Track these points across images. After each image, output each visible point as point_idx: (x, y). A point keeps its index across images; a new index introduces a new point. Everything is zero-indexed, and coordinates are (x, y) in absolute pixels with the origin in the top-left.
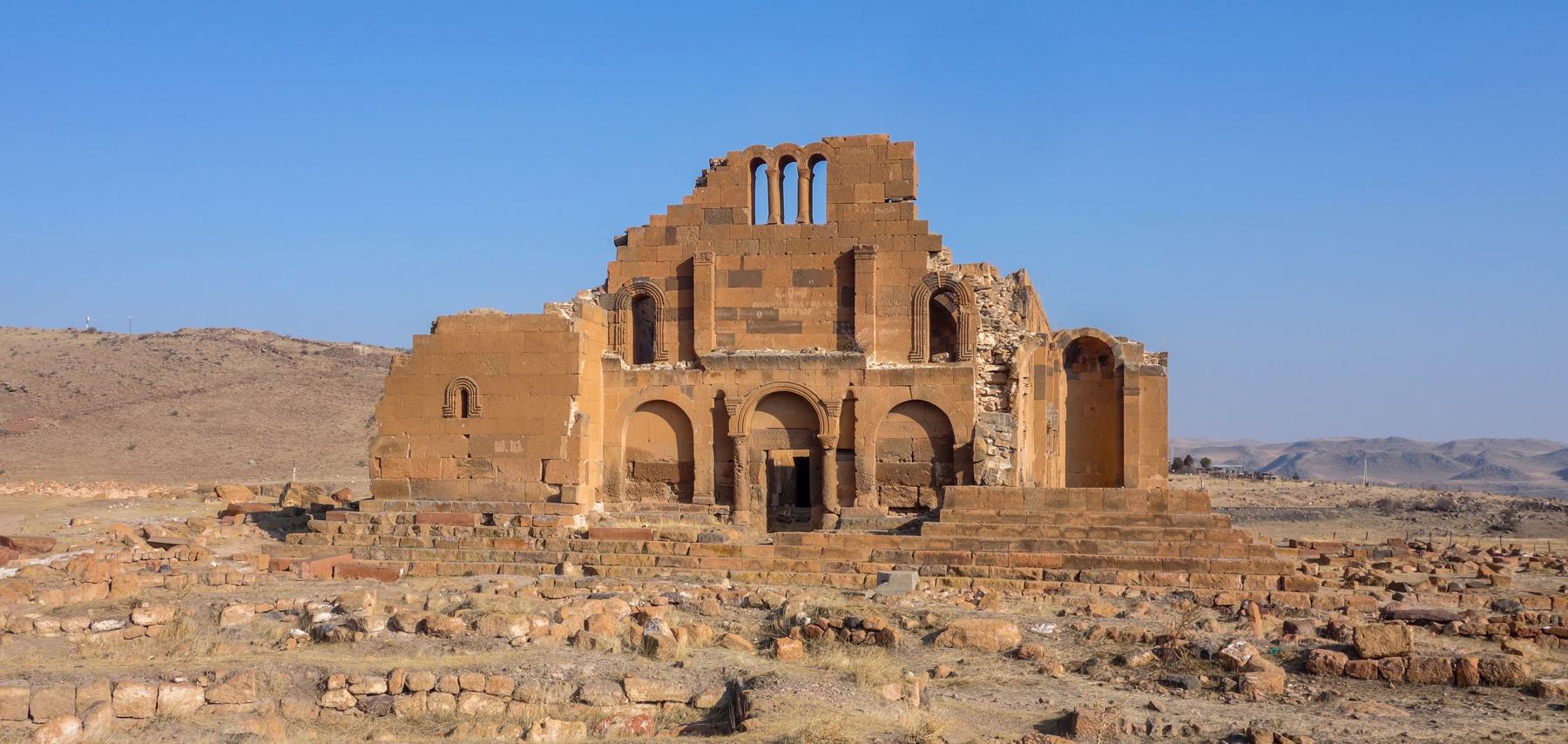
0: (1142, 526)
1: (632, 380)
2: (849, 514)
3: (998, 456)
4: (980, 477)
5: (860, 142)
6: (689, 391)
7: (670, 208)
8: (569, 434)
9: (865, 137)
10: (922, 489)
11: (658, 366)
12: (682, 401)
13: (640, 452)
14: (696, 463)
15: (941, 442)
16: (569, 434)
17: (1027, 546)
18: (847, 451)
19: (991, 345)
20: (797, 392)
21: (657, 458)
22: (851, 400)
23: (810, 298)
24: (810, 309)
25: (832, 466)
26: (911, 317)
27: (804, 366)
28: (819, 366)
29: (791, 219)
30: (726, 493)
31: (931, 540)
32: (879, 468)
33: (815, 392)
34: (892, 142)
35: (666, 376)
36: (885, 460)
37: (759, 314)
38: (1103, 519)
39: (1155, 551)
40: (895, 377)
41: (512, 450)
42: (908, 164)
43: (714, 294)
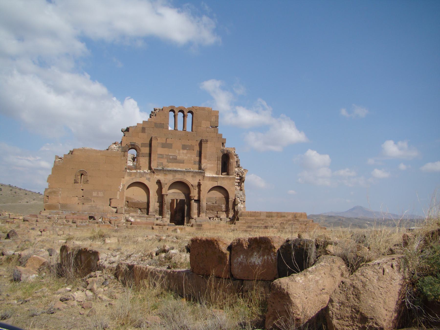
1: (130, 175)
2: (198, 219)
3: (240, 203)
4: (236, 209)
5: (203, 109)
6: (149, 179)
7: (143, 121)
8: (120, 191)
9: (205, 107)
11: (139, 171)
12: (146, 183)
13: (130, 198)
16: (120, 191)
18: (198, 201)
19: (236, 171)
20: (185, 182)
21: (136, 201)
24: (187, 157)
25: (194, 205)
26: (217, 161)
27: (186, 174)
28: (191, 174)
30: (161, 213)
31: (240, 226)
33: (190, 182)
34: (213, 110)
35: (141, 174)
37: (171, 157)
38: (283, 220)
40: (213, 179)
41: (99, 195)
42: (217, 117)
43: (158, 150)
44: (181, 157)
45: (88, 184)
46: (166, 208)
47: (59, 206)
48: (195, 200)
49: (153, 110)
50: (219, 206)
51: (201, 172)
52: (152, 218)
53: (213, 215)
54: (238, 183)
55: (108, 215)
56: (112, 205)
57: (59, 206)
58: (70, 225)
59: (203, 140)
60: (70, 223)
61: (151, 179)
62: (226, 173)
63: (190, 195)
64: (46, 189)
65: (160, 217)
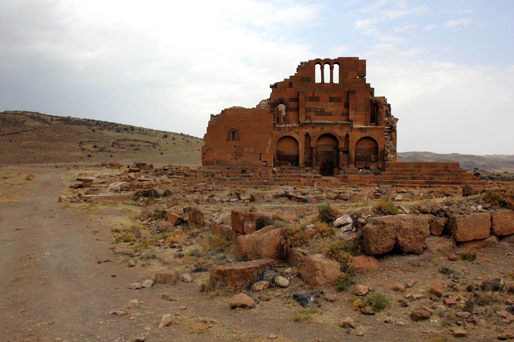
0: (443, 172)
6: (297, 133)
7: (290, 77)
10: (368, 163)
11: (288, 125)
12: (295, 136)
13: (281, 152)
14: (300, 155)
15: (374, 149)
17: (414, 178)
18: (347, 152)
21: (286, 154)
22: (347, 136)
23: (334, 106)
26: (365, 112)
27: (334, 126)
28: (339, 126)
29: (327, 80)
32: (355, 156)
34: (360, 59)
36: (357, 154)
37: (319, 110)
38: (432, 170)
39: (449, 179)
40: (361, 130)
41: (250, 151)
44: (328, 109)
45: (240, 140)
46: (315, 160)
47: (215, 162)
48: (344, 152)
49: (300, 64)
50: (368, 156)
51: (348, 123)
52: (302, 170)
53: (362, 166)
54: (389, 132)
55: (259, 169)
56: (261, 159)
57: (215, 162)
58: (225, 178)
59: (350, 91)
60: (225, 177)
61: (300, 132)
62: (375, 123)
63: (339, 147)
64: (203, 147)
65: (310, 168)
